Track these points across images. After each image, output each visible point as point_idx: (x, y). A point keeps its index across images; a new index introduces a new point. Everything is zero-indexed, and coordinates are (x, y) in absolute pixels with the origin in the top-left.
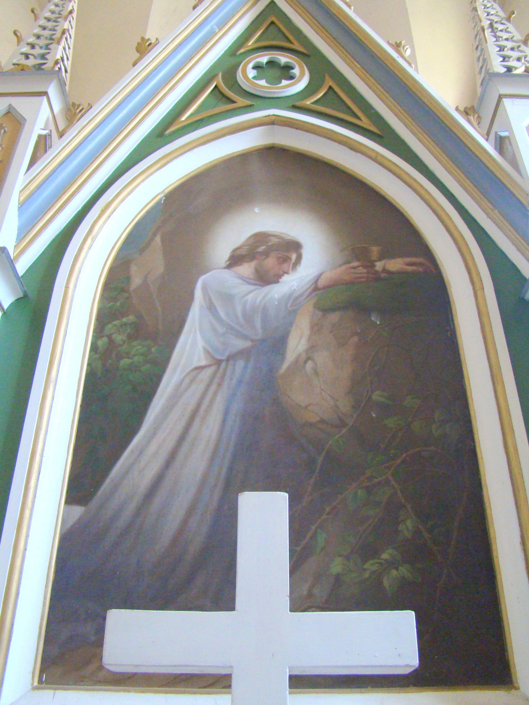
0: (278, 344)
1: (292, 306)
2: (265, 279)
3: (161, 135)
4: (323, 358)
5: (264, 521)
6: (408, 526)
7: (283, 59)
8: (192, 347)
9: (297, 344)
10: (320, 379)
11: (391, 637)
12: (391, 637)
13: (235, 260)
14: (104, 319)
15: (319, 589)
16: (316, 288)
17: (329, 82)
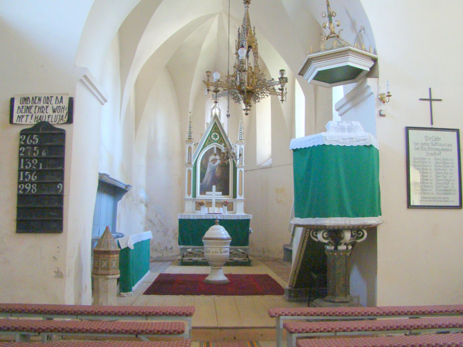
0: (214, 170)
1: (216, 166)
2: (214, 163)
3: (204, 146)
4: (218, 171)
5: (214, 187)
6: (224, 185)
7: (217, 134)
8: (208, 170)
9: (217, 170)
10: (218, 173)
11: (221, 193)
12: (221, 193)
13: (212, 161)
14: (201, 167)
15: (217, 190)
16: (219, 164)
17: (221, 138)
